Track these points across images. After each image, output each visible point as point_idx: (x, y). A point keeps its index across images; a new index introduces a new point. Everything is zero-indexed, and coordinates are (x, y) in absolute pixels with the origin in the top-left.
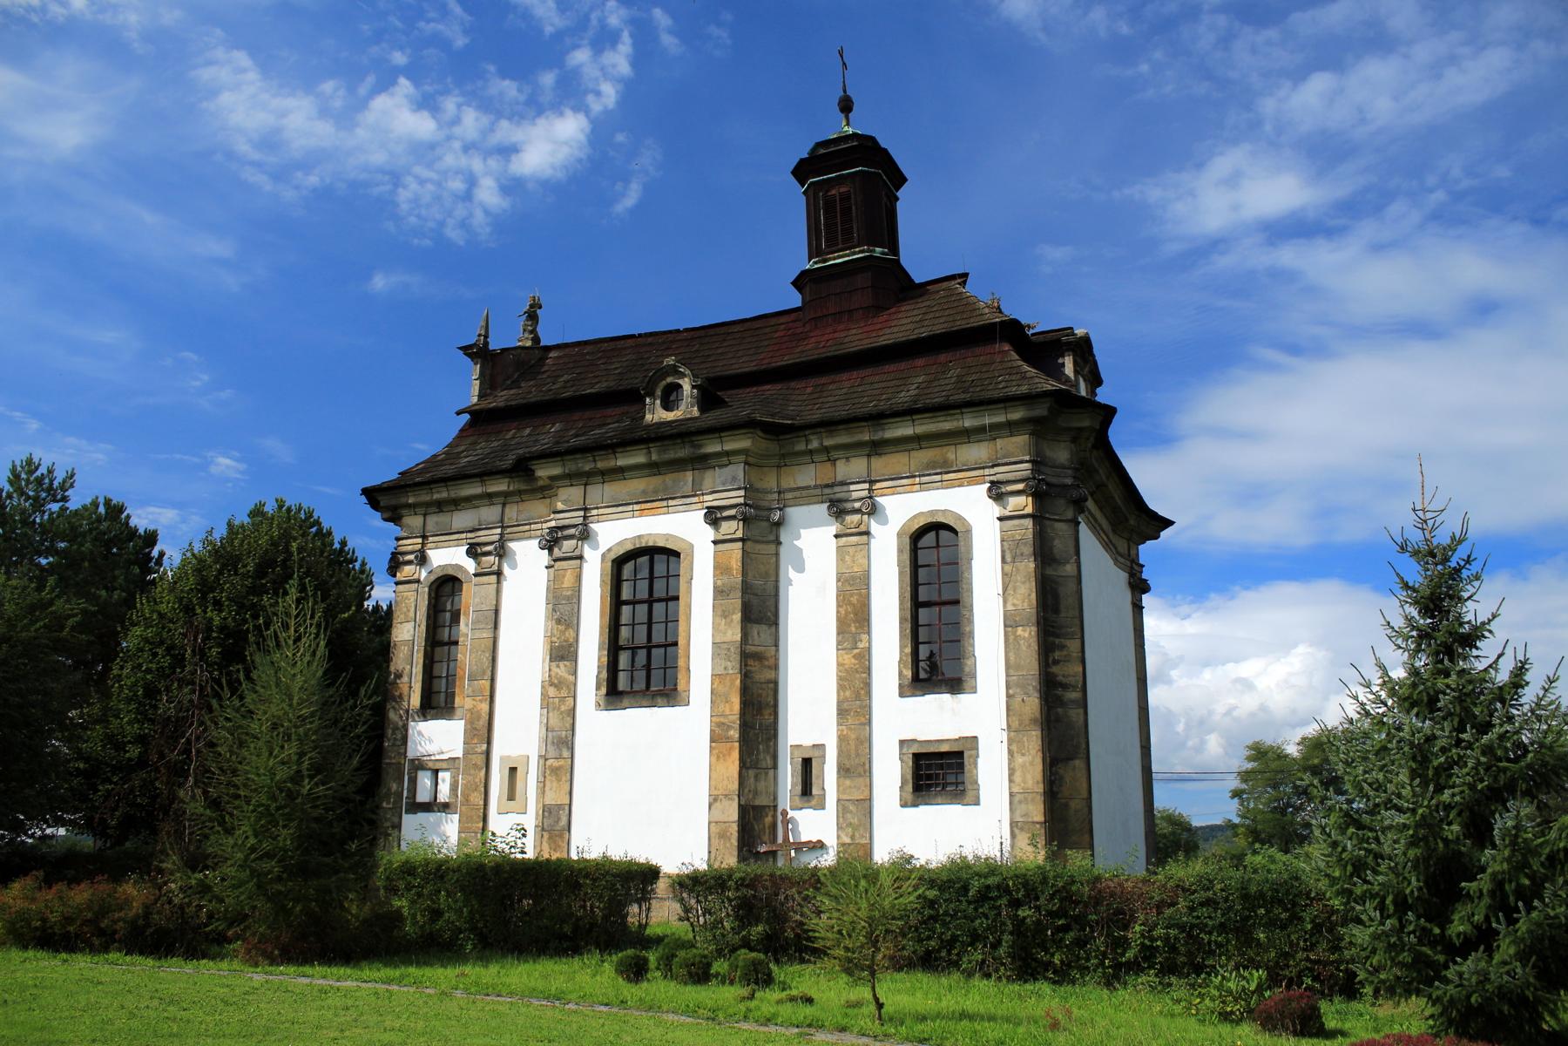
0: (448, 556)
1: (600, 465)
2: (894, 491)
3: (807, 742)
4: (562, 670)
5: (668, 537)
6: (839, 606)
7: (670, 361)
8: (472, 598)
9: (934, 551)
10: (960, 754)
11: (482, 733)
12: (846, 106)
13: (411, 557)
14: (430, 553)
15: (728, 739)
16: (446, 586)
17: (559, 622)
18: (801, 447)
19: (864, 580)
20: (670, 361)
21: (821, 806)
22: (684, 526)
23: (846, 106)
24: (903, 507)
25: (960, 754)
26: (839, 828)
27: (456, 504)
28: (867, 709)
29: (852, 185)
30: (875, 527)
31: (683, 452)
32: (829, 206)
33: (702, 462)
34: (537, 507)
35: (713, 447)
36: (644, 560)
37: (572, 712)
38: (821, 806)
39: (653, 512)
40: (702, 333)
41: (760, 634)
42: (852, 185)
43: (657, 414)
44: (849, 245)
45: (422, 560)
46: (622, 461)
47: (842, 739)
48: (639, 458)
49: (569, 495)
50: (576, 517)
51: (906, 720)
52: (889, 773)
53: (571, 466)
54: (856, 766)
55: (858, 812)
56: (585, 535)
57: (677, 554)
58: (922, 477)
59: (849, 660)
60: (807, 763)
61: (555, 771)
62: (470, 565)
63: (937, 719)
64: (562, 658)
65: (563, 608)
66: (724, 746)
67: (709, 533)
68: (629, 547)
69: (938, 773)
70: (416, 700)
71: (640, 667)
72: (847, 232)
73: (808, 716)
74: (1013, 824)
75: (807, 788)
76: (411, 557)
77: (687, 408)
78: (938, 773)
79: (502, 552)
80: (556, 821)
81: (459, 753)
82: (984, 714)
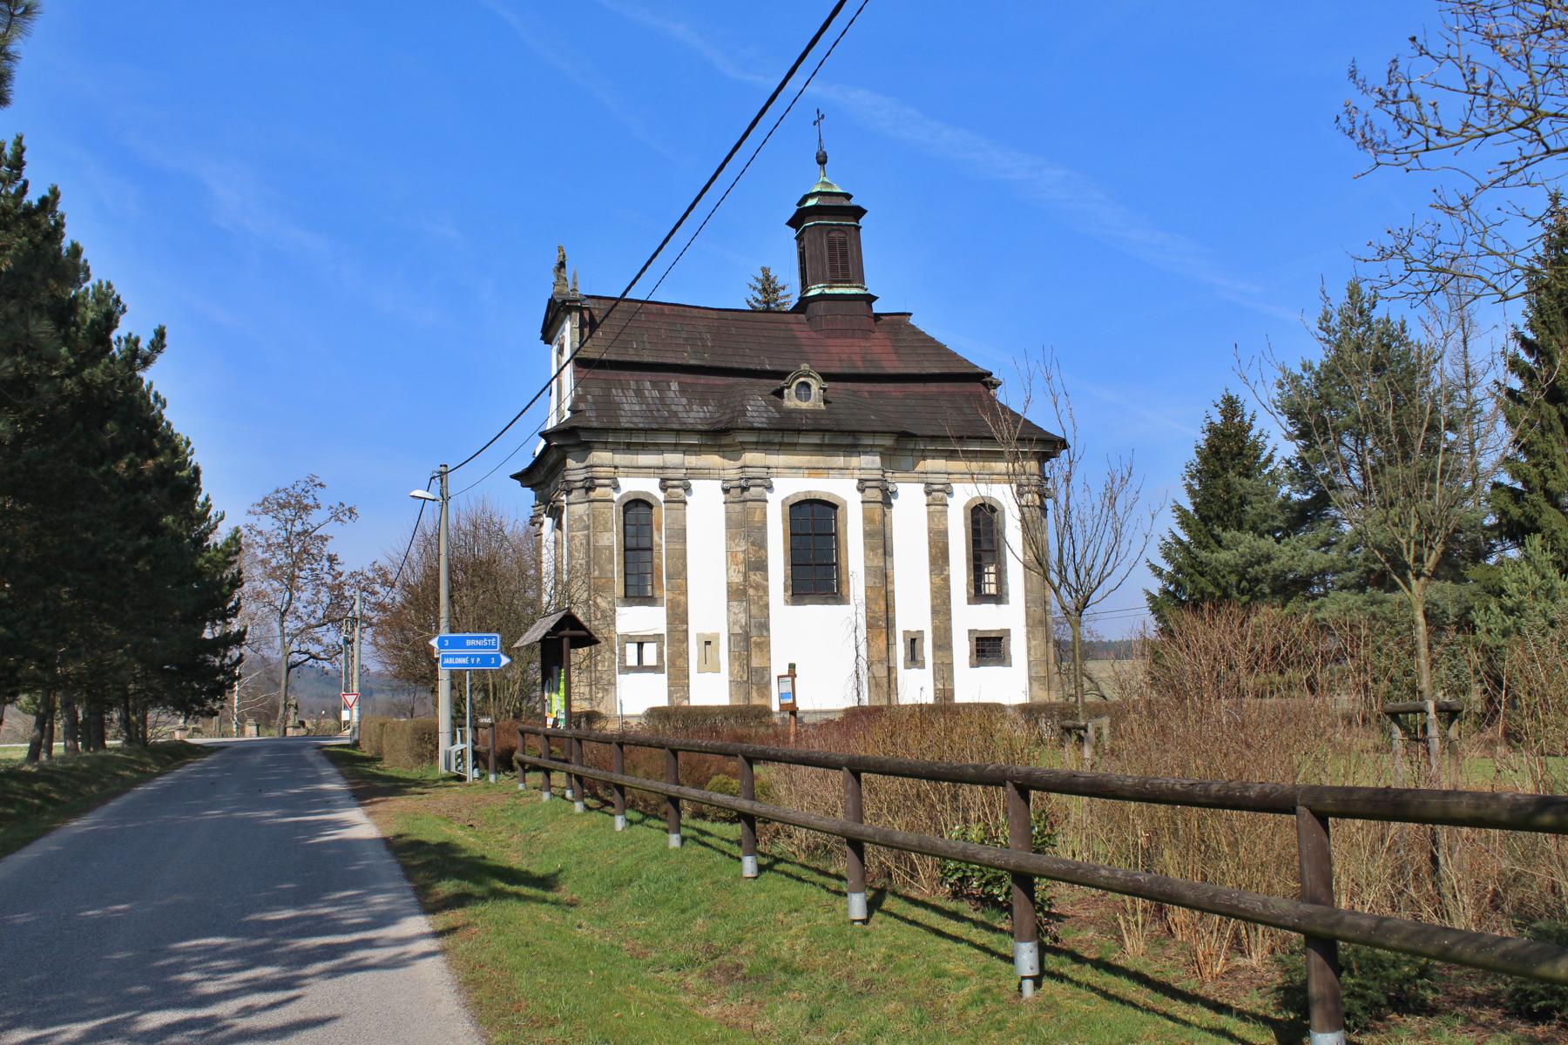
0: (648, 486)
1: (786, 440)
2: (961, 481)
3: (914, 629)
4: (755, 577)
5: (830, 494)
6: (930, 548)
7: (805, 367)
8: (662, 515)
9: (983, 520)
10: (1000, 639)
11: (678, 617)
12: (822, 160)
13: (607, 482)
14: (621, 481)
15: (879, 627)
16: (637, 506)
17: (753, 544)
18: (911, 446)
19: (945, 533)
20: (805, 367)
21: (923, 667)
22: (841, 485)
23: (822, 160)
24: (963, 495)
25: (1000, 639)
26: (935, 679)
27: (643, 448)
28: (949, 610)
29: (828, 227)
30: (949, 501)
31: (848, 440)
32: (831, 247)
33: (853, 449)
34: (713, 460)
35: (868, 441)
36: (808, 508)
37: (767, 606)
38: (923, 667)
39: (818, 476)
40: (715, 315)
41: (879, 562)
42: (828, 227)
43: (791, 401)
44: (847, 281)
45: (616, 488)
46: (802, 440)
47: (935, 629)
48: (815, 439)
49: (750, 457)
50: (762, 472)
51: (969, 618)
52: (962, 649)
53: (763, 437)
54: (943, 643)
55: (944, 671)
56: (770, 488)
57: (835, 507)
58: (973, 477)
59: (938, 580)
60: (913, 641)
61: (758, 645)
62: (661, 496)
63: (988, 618)
64: (758, 569)
65: (745, 529)
66: (876, 631)
67: (859, 497)
68: (803, 498)
69: (989, 648)
70: (619, 589)
71: (815, 575)
72: (845, 268)
73: (912, 612)
74: (1030, 678)
75: (914, 659)
76: (607, 482)
77: (814, 402)
78: (989, 648)
79: (687, 489)
80: (751, 675)
81: (663, 629)
82: (1010, 617)
